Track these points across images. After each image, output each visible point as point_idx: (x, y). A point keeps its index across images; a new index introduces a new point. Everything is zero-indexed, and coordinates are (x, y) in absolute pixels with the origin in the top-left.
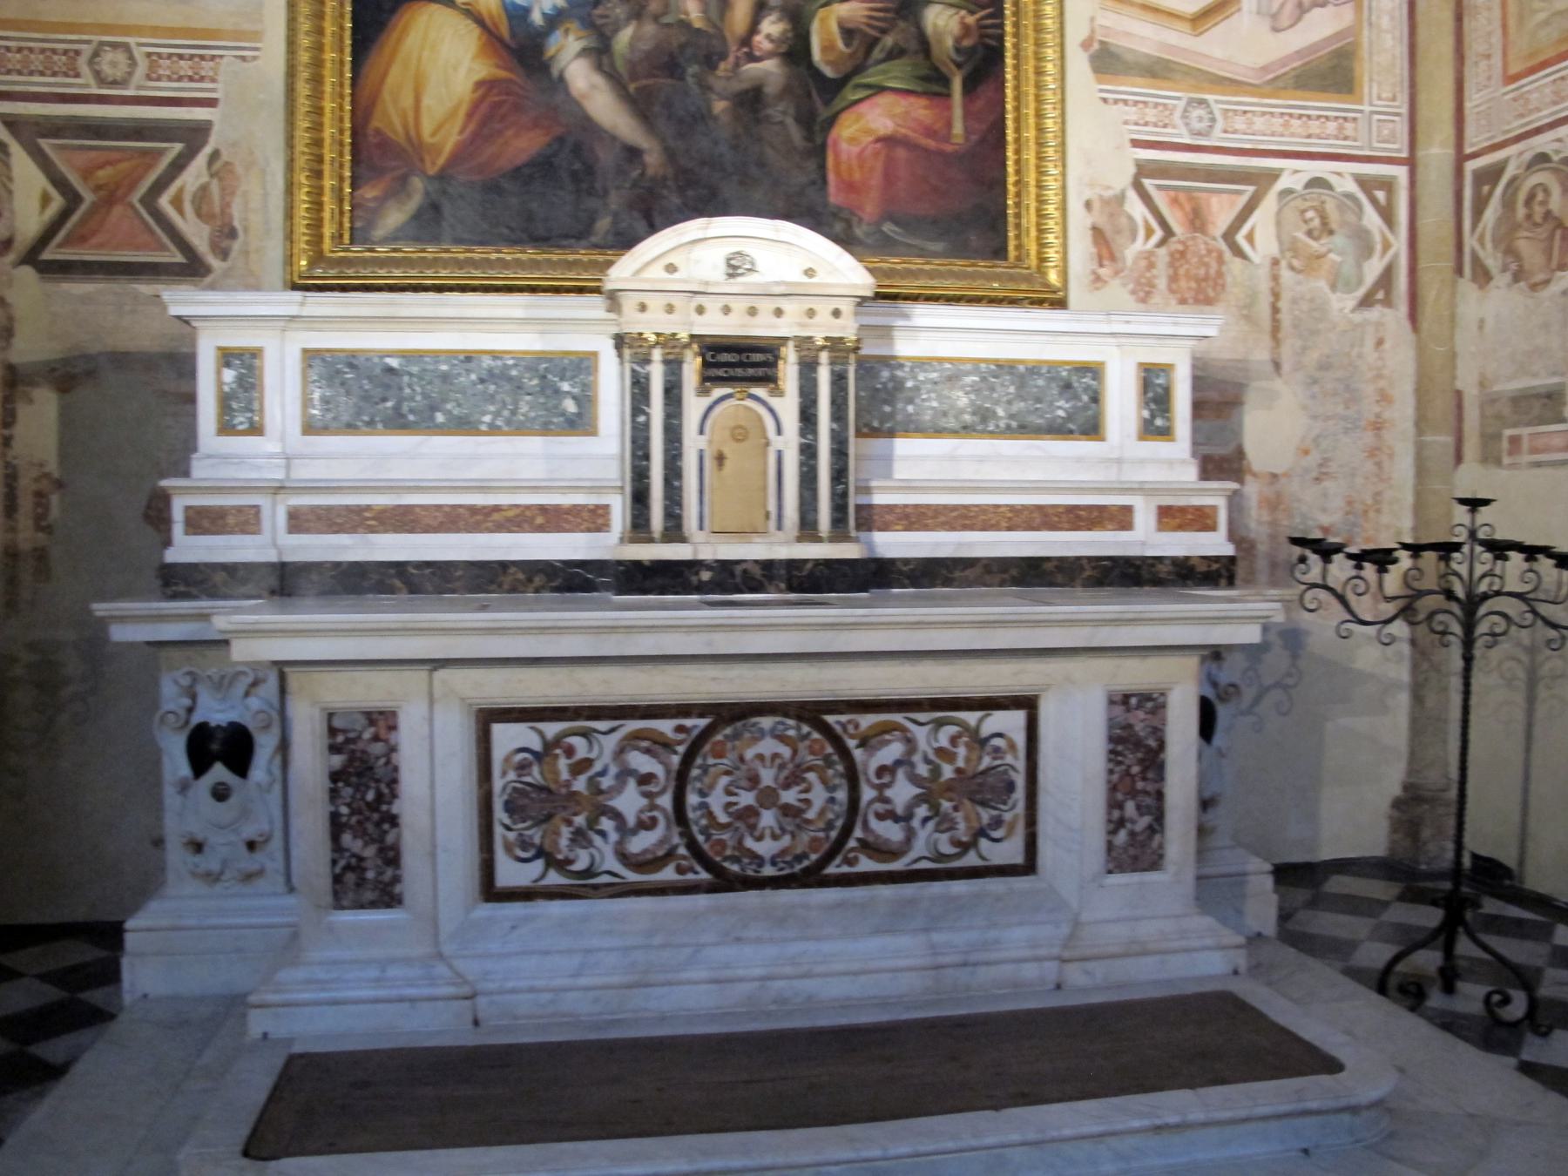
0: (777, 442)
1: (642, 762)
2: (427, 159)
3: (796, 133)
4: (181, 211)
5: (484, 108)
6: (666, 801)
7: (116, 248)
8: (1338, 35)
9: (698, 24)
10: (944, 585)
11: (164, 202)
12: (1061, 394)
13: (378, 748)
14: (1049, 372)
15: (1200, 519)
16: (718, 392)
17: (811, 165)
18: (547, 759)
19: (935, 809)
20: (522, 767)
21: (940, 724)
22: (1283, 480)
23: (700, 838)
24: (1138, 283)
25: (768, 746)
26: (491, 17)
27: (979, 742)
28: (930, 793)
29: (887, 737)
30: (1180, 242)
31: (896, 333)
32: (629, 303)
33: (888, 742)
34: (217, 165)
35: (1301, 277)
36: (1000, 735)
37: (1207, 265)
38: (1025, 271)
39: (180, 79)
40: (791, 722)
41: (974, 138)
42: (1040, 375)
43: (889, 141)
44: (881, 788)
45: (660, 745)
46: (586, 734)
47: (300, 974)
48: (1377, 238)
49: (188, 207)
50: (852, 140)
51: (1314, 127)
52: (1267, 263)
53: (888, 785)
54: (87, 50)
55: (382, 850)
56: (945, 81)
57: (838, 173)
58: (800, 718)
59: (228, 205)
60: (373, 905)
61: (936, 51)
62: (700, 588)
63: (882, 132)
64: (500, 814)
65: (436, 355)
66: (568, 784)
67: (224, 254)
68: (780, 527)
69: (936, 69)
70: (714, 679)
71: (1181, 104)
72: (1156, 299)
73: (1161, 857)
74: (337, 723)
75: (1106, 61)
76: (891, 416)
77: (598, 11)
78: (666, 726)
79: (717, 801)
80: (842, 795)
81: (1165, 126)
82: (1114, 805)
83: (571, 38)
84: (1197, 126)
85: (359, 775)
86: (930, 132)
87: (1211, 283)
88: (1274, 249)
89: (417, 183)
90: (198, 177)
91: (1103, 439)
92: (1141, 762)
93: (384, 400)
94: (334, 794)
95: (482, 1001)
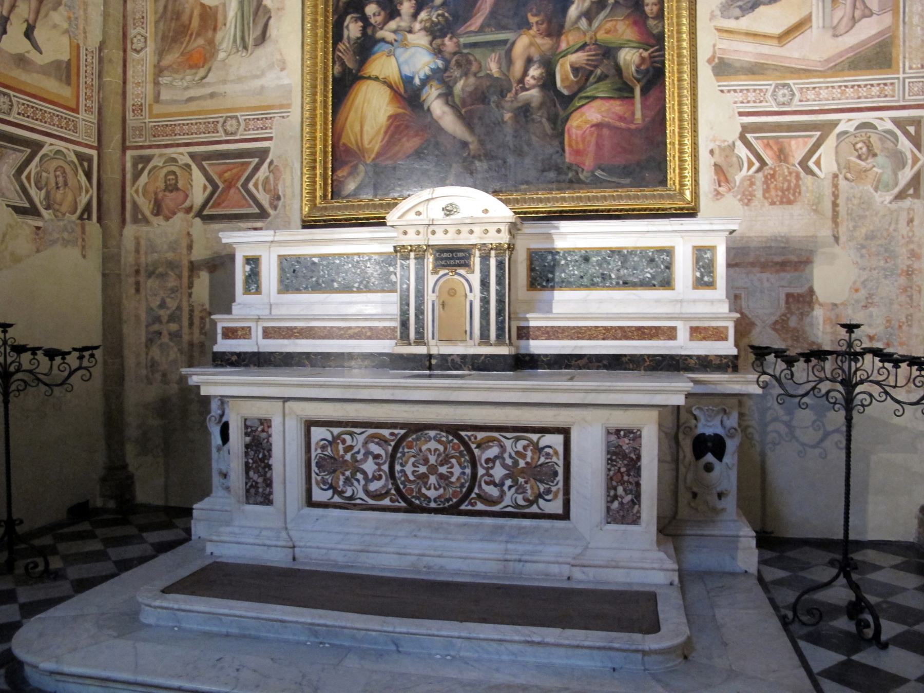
0: (470, 296)
1: (375, 449)
2: (366, 155)
3: (547, 126)
5: (392, 128)
6: (386, 467)
7: (232, 208)
8: (880, 33)
9: (496, 75)
10: (566, 368)
12: (647, 265)
13: (264, 435)
14: (640, 253)
15: (718, 335)
16: (442, 272)
17: (556, 143)
18: (334, 445)
19: (516, 482)
20: (324, 448)
21: (518, 439)
22: (841, 307)
23: (401, 487)
24: (744, 194)
25: (433, 445)
26: (395, 83)
27: (538, 450)
28: (513, 473)
29: (491, 444)
30: (771, 168)
31: (554, 236)
33: (492, 447)
34: (272, 168)
35: (853, 184)
36: (550, 447)
37: (789, 182)
38: (671, 193)
39: (257, 129)
40: (444, 434)
41: (647, 119)
42: (636, 255)
43: (598, 126)
44: (488, 469)
45: (383, 441)
46: (351, 434)
47: (229, 529)
48: (909, 156)
49: (260, 187)
50: (578, 127)
51: (863, 92)
52: (830, 177)
53: (492, 468)
54: (221, 120)
55: (265, 480)
56: (632, 90)
57: (570, 146)
58: (448, 432)
59: (277, 185)
60: (261, 503)
61: (625, 74)
64: (314, 468)
66: (343, 457)
67: (275, 208)
68: (471, 338)
69: (625, 83)
70: (405, 411)
71: (771, 89)
72: (755, 203)
73: (639, 518)
74: (248, 423)
75: (723, 68)
76: (553, 279)
77: (446, 75)
78: (386, 432)
79: (409, 469)
80: (468, 471)
81: (761, 102)
82: (610, 487)
83: (433, 89)
84: (781, 99)
85: (257, 446)
86: (621, 118)
87: (791, 191)
88: (835, 168)
90: (264, 173)
91: (673, 289)
92: (626, 465)
93: (312, 277)
94: (246, 454)
95: (297, 549)
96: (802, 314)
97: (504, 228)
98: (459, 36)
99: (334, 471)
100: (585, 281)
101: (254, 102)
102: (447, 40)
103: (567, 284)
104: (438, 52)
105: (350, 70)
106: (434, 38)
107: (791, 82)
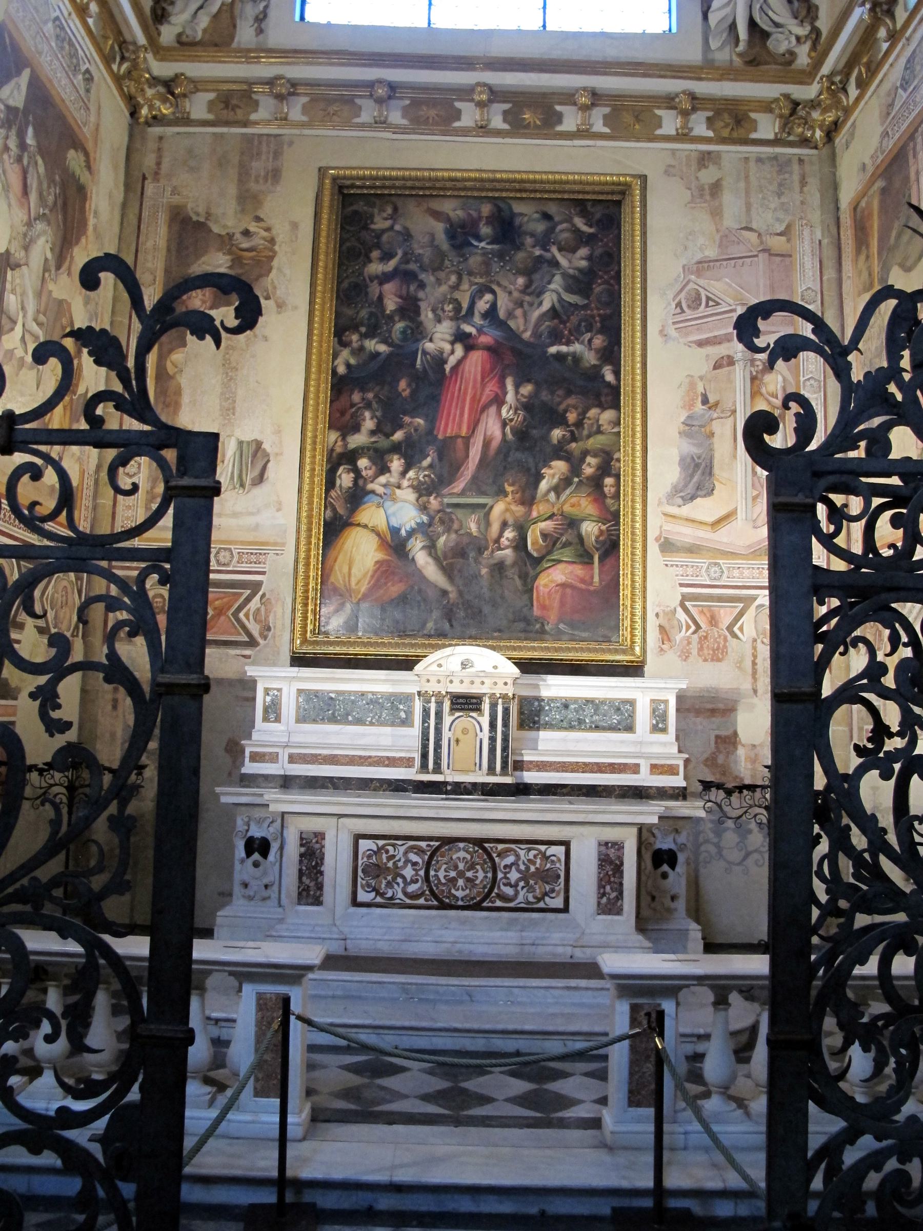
0: (480, 735)
1: (413, 857)
3: (518, 582)
4: (248, 619)
5: (379, 573)
6: (422, 873)
11: (241, 615)
13: (317, 846)
15: (671, 770)
16: (457, 714)
17: (526, 597)
19: (527, 883)
20: (369, 857)
21: (529, 850)
25: (462, 854)
27: (545, 858)
28: (525, 876)
32: (424, 680)
37: (719, 643)
43: (563, 585)
44: (505, 873)
45: (420, 851)
46: (394, 845)
47: (284, 926)
49: (251, 617)
50: (545, 586)
55: (316, 884)
56: (592, 558)
58: (474, 844)
60: (312, 904)
62: (446, 793)
63: (559, 582)
64: (360, 873)
65: (350, 692)
67: (265, 638)
69: (586, 551)
71: (705, 566)
72: (691, 659)
75: (667, 546)
76: (538, 722)
78: (423, 844)
80: (490, 875)
82: (601, 886)
84: (713, 575)
86: (582, 581)
88: (754, 634)
89: (348, 607)
94: (301, 862)
95: (348, 942)
96: (728, 753)
97: (510, 681)
98: (443, 496)
99: (378, 876)
100: (565, 724)
101: (250, 537)
102: (432, 498)
103: (549, 726)
104: (424, 508)
105: (341, 516)
106: (420, 496)
107: (721, 562)
